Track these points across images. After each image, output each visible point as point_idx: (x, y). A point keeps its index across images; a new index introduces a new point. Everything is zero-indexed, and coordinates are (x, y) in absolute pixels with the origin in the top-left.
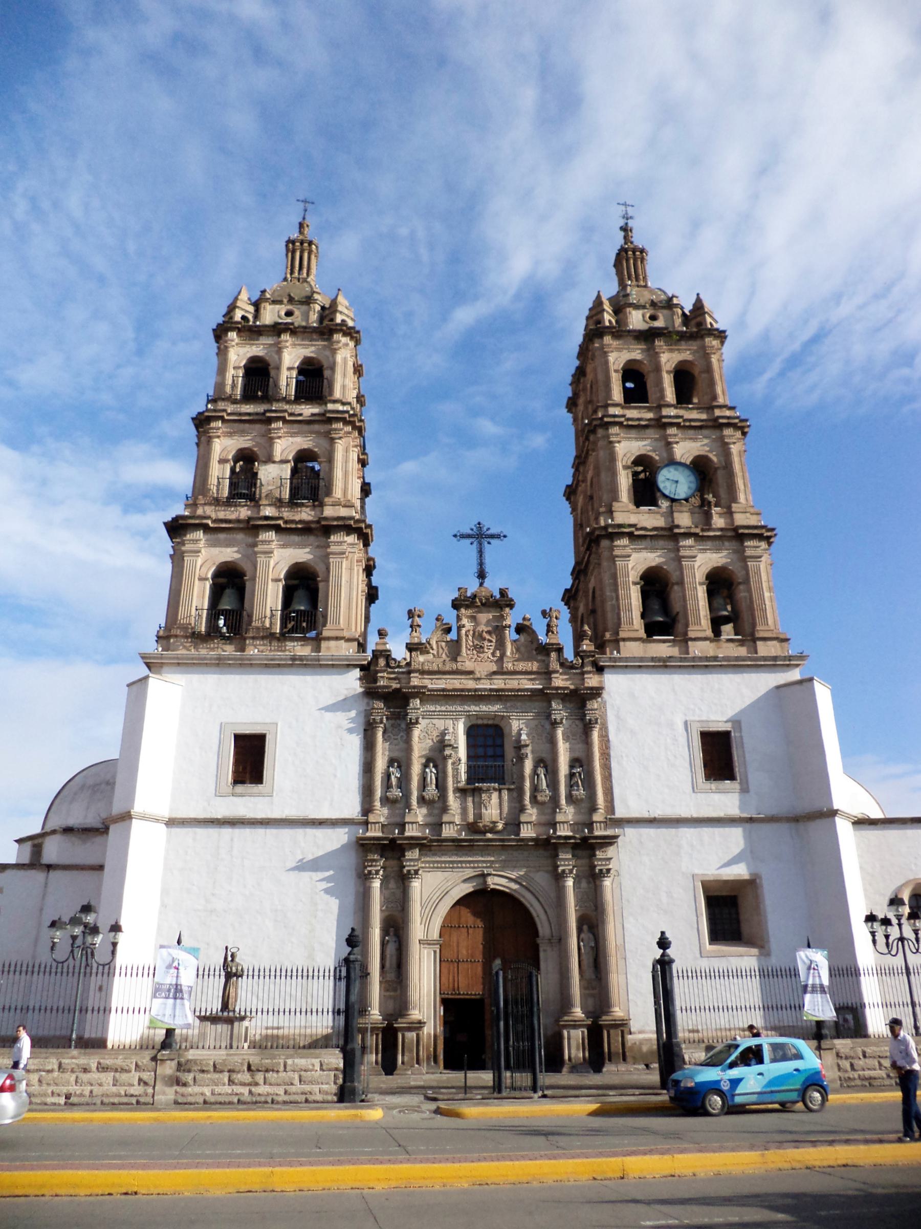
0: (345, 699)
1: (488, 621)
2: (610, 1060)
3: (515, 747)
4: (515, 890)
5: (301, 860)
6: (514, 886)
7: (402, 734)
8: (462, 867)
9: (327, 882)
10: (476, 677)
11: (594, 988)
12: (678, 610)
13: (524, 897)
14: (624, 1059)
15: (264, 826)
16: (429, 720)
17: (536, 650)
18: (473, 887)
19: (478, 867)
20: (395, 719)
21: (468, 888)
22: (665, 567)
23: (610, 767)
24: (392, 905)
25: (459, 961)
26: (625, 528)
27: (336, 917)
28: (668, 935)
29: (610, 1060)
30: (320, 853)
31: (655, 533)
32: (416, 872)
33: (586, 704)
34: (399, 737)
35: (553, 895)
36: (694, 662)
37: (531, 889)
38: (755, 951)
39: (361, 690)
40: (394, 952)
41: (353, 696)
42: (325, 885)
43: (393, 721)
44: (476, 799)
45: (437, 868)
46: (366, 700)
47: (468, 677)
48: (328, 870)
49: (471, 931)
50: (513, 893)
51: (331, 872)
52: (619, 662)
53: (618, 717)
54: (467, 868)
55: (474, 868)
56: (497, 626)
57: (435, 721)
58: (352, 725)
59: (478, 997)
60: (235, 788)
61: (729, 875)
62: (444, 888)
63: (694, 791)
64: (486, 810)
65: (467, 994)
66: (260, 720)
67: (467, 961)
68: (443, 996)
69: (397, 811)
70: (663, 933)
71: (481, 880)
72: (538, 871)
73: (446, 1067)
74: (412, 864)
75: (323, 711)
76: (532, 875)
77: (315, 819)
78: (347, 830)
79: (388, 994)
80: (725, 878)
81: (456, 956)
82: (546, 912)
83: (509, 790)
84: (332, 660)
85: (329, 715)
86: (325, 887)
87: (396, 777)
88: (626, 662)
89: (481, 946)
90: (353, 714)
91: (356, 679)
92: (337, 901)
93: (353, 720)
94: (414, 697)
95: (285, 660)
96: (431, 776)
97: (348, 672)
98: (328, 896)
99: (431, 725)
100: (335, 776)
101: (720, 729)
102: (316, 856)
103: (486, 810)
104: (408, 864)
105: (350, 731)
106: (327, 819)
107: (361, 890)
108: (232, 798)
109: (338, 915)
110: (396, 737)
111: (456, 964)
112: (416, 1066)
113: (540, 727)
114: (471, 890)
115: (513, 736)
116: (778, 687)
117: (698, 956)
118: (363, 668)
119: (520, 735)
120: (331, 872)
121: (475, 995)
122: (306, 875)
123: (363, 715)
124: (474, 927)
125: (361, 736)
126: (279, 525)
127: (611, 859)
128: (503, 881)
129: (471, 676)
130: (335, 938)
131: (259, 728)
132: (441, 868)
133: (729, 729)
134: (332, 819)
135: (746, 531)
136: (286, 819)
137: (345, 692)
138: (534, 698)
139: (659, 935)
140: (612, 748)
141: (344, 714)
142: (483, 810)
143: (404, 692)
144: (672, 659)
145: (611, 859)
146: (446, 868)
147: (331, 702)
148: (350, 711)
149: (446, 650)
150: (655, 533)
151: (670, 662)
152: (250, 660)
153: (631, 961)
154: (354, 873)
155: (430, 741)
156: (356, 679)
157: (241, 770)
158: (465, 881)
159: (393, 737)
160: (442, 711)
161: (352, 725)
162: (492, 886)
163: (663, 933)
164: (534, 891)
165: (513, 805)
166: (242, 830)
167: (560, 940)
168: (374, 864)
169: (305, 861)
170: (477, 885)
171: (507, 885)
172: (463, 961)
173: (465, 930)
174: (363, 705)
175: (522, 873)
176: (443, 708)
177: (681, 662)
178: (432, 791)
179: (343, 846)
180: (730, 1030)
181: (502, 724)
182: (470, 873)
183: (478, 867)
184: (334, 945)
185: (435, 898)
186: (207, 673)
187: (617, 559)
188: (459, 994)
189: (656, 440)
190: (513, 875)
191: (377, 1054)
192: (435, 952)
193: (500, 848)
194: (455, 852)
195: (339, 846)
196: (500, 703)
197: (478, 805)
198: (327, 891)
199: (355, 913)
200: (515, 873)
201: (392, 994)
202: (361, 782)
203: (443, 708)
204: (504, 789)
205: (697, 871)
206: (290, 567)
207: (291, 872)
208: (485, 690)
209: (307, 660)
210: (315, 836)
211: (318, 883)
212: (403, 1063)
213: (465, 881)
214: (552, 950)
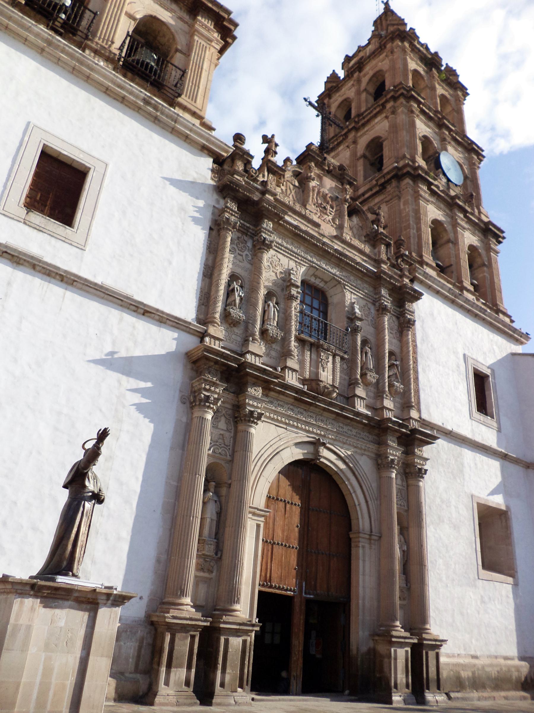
0: (192, 183)
1: (331, 188)
2: (428, 689)
3: (348, 318)
4: (341, 470)
5: (112, 353)
6: (342, 466)
7: (246, 252)
8: (297, 427)
9: (142, 397)
10: (321, 232)
11: (404, 599)
12: (452, 263)
13: (348, 480)
14: (439, 688)
15: (65, 285)
16: (275, 252)
17: (365, 237)
18: (304, 454)
19: (313, 433)
20: (243, 233)
21: (298, 454)
22: (445, 225)
23: (417, 371)
24: (220, 451)
25: (274, 543)
26: (429, 177)
27: (147, 449)
29: (428, 689)
30: (138, 353)
31: (443, 195)
32: (260, 416)
33: (405, 304)
34: (244, 254)
35: (374, 485)
36: (472, 307)
37: (356, 473)
38: (510, 580)
39: (212, 183)
40: (215, 517)
41: (202, 184)
42: (138, 399)
43: (240, 235)
44: (314, 356)
45: (273, 419)
46: (215, 196)
47: (314, 228)
48: (145, 381)
49: (288, 506)
50: (339, 472)
51: (149, 385)
52: (429, 280)
53: (422, 327)
54: (301, 429)
55: (308, 432)
56: (337, 197)
57: (280, 256)
58: (197, 215)
59: (289, 593)
60: (30, 213)
61: (493, 502)
62: (275, 447)
63: (470, 418)
64: (324, 371)
65: (279, 588)
66: (85, 148)
67: (282, 545)
68: (263, 589)
69: (233, 336)
71: (311, 448)
72: (362, 455)
73: (252, 690)
74: (255, 404)
75: (168, 183)
76: (358, 457)
77: (142, 303)
78: (176, 335)
79: (201, 574)
80: (491, 504)
81: (270, 537)
82: (367, 502)
83: (342, 358)
84: (191, 130)
85: (172, 190)
86: (137, 401)
87: (239, 295)
88: (433, 282)
89: (297, 530)
90: (201, 203)
91: (209, 169)
92: (152, 425)
93: (199, 210)
94: (270, 219)
95: (137, 97)
96: (274, 311)
97: (201, 156)
98: (141, 416)
99: (275, 258)
100: (170, 263)
101: (484, 372)
102: (129, 355)
103: (324, 371)
104: (251, 402)
105: (195, 220)
106: (158, 310)
107: (184, 420)
108: (21, 225)
109: (151, 446)
110: (240, 253)
111: (270, 546)
112: (239, 690)
113: (366, 308)
114: (301, 457)
115: (346, 307)
116: (514, 354)
117: (477, 577)
118: (218, 160)
119: (353, 308)
120: (149, 385)
121: (287, 590)
122: (113, 377)
123: (211, 210)
124: (292, 504)
125: (207, 231)
127: (427, 459)
128: (333, 457)
129: (316, 229)
130: (141, 478)
131: (81, 156)
132: (277, 421)
133: (489, 374)
134: (163, 312)
135: (493, 229)
136: (101, 287)
137: (195, 175)
138: (366, 279)
140: (418, 353)
141: (190, 197)
142: (321, 370)
143: (264, 206)
144: (460, 297)
145: (427, 459)
146: (281, 422)
147: (177, 176)
148: (197, 198)
149: (293, 192)
150: (443, 195)
151: (459, 299)
152: (92, 69)
153: (432, 574)
154: (177, 395)
155: (274, 274)
156: (209, 169)
157: (38, 198)
158: (297, 444)
159: (238, 251)
160: (288, 249)
161: (197, 215)
162: (322, 460)
164: (358, 476)
165: (344, 376)
166: (29, 277)
167: (380, 537)
168: (213, 388)
169: (116, 356)
170: (307, 453)
171: (335, 461)
172: (278, 544)
173: (282, 505)
174: (213, 198)
175: (349, 453)
176: (289, 247)
177: (465, 302)
178: (272, 327)
179: (168, 353)
181: (330, 293)
182: (303, 437)
183: (313, 433)
184: (138, 490)
185: (266, 456)
186: (24, 53)
187: (421, 198)
188: (271, 587)
189: (435, 132)
190: (343, 452)
191: (189, 668)
192: (258, 526)
193: (334, 416)
194: (291, 407)
195: (163, 352)
196: (337, 269)
197: (317, 363)
198: (139, 407)
199: (172, 448)
200: (343, 451)
201: (206, 575)
202: (200, 285)
203: (289, 247)
204: (339, 355)
205: (476, 493)
206: (145, 16)
207: (92, 365)
208: (332, 248)
209: (162, 113)
210: (134, 327)
211: (128, 392)
212: (222, 685)
213: (297, 444)
214: (370, 548)
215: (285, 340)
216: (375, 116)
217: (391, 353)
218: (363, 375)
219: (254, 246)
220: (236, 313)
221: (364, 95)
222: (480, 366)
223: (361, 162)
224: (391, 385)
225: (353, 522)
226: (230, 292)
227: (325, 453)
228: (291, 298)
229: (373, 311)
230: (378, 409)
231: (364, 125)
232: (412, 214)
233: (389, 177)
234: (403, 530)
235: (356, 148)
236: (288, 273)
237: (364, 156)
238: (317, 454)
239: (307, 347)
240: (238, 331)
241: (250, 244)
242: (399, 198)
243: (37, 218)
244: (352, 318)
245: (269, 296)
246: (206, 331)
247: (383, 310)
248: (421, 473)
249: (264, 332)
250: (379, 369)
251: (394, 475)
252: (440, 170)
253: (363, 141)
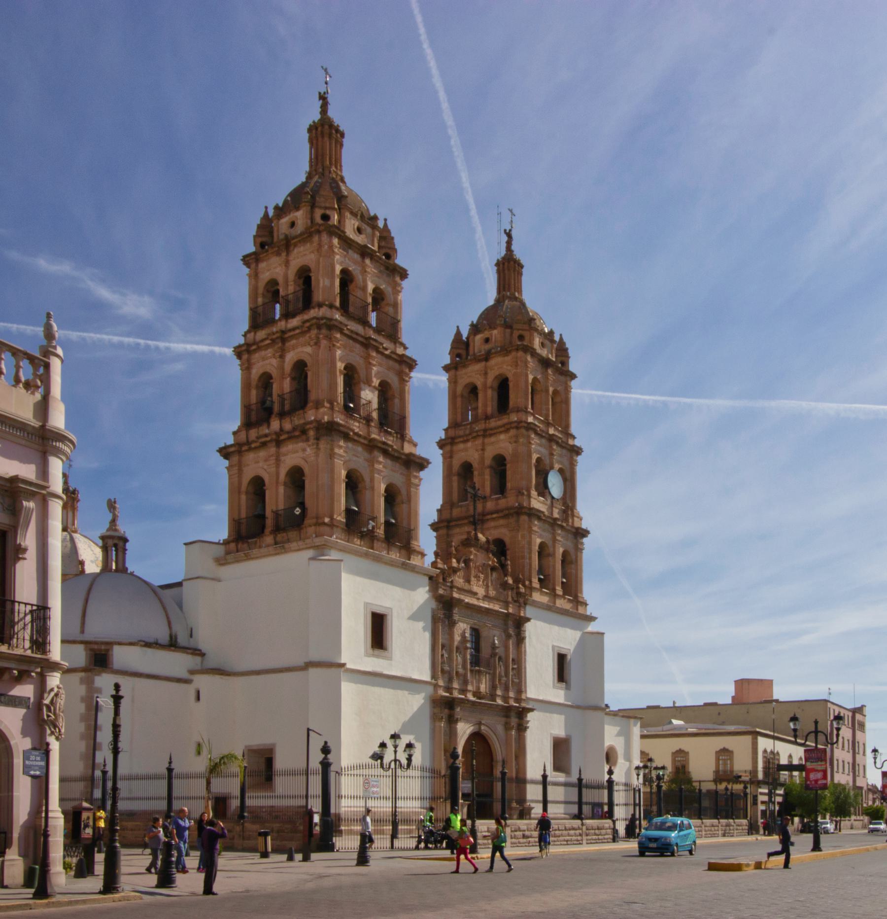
28: (329, 744)
32: (461, 719)
70: (326, 743)
126: (388, 450)
139: (323, 744)
163: (326, 743)
180: (383, 807)
197: (479, 681)
215: (465, 675)
216: (501, 432)
217: (513, 660)
218: (500, 680)
219: (449, 623)
220: (447, 668)
221: (489, 392)
222: (562, 650)
223: (487, 471)
224: (513, 681)
225: (494, 757)
226: (442, 655)
227: (483, 727)
228: (466, 648)
229: (504, 637)
230: (506, 698)
231: (491, 435)
232: (526, 546)
233: (512, 511)
234: (517, 757)
235: (484, 454)
236: (464, 632)
237: (491, 467)
238: (480, 728)
239: (474, 673)
240: (446, 675)
241: (447, 622)
242: (518, 531)
243: (377, 652)
244: (494, 647)
245: (457, 648)
246: (437, 683)
247: (508, 636)
248: (526, 728)
249: (457, 673)
250: (507, 675)
251: (513, 733)
252: (547, 491)
253: (490, 452)
